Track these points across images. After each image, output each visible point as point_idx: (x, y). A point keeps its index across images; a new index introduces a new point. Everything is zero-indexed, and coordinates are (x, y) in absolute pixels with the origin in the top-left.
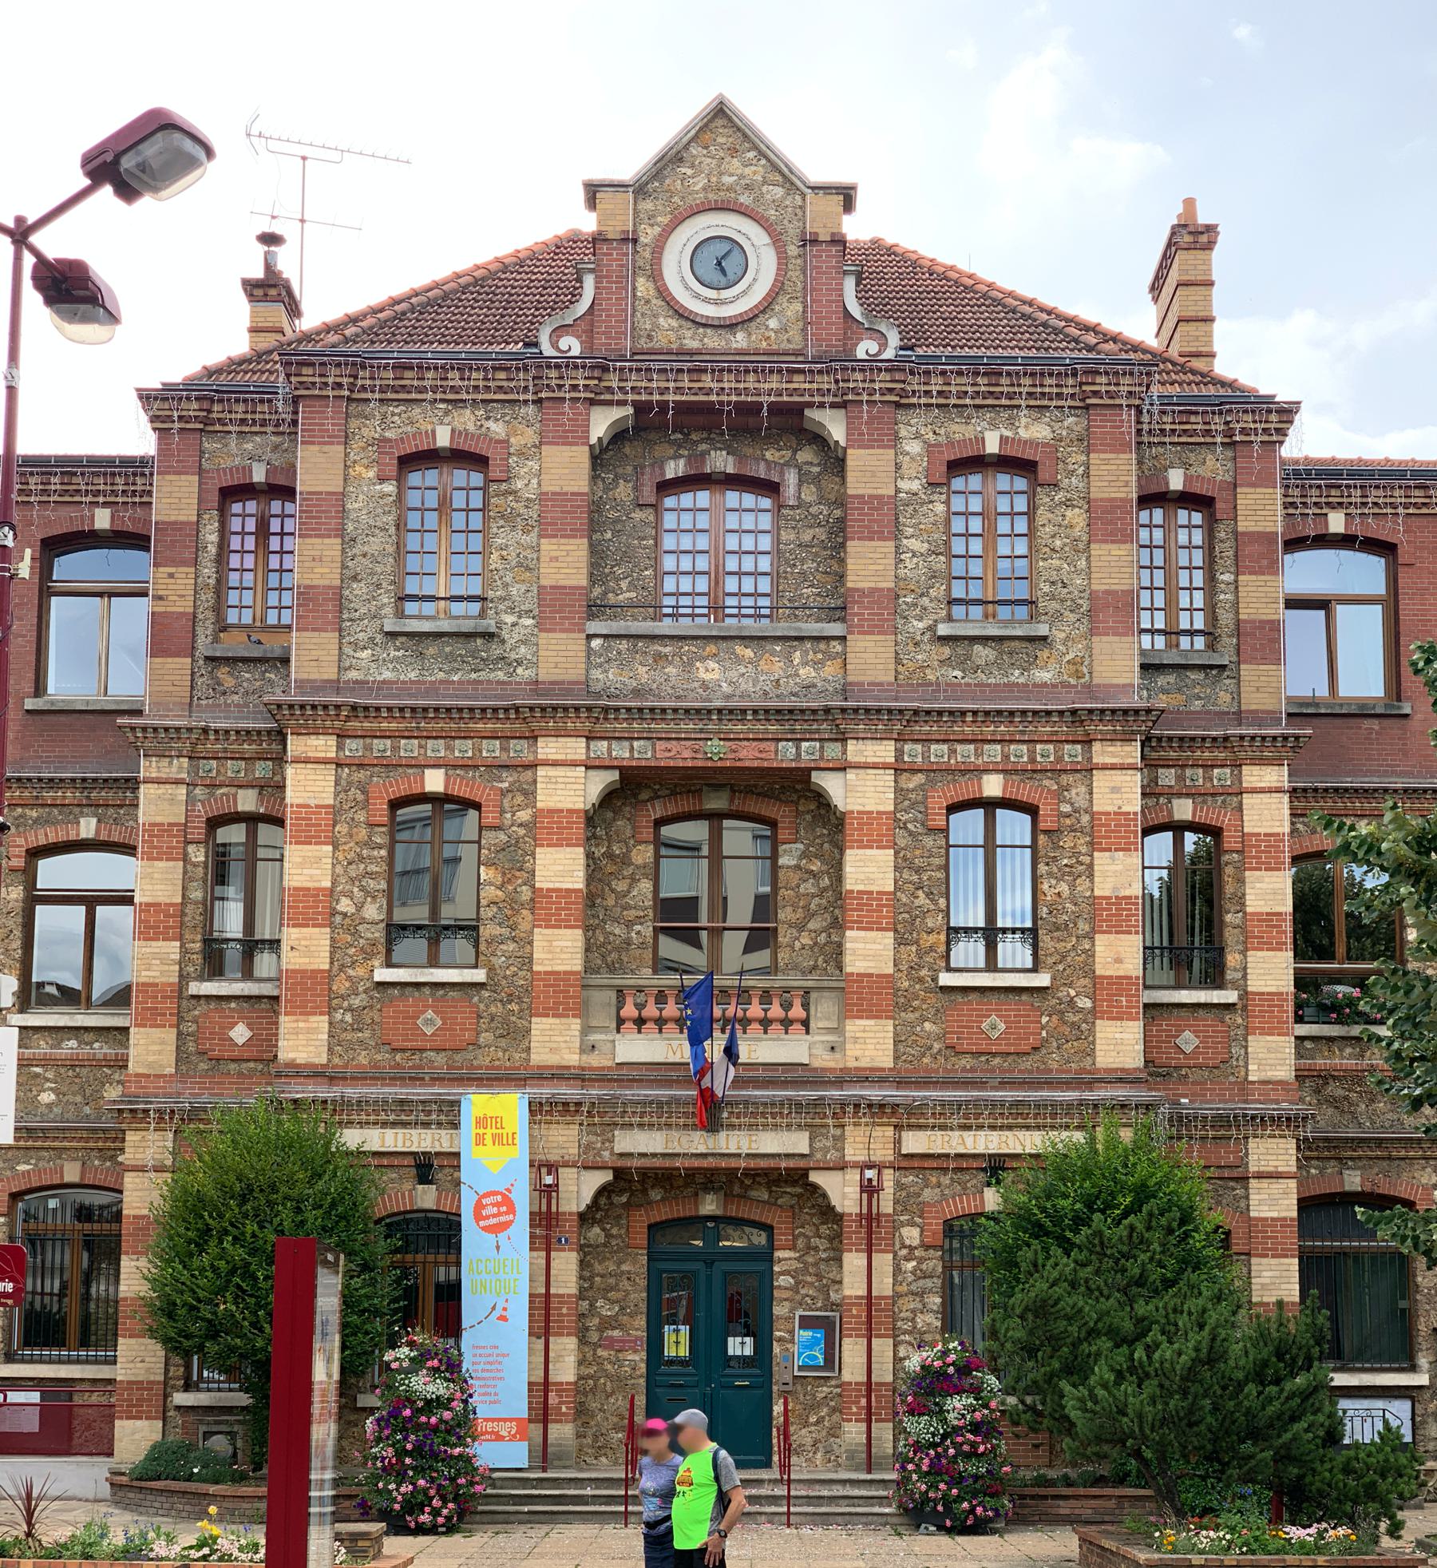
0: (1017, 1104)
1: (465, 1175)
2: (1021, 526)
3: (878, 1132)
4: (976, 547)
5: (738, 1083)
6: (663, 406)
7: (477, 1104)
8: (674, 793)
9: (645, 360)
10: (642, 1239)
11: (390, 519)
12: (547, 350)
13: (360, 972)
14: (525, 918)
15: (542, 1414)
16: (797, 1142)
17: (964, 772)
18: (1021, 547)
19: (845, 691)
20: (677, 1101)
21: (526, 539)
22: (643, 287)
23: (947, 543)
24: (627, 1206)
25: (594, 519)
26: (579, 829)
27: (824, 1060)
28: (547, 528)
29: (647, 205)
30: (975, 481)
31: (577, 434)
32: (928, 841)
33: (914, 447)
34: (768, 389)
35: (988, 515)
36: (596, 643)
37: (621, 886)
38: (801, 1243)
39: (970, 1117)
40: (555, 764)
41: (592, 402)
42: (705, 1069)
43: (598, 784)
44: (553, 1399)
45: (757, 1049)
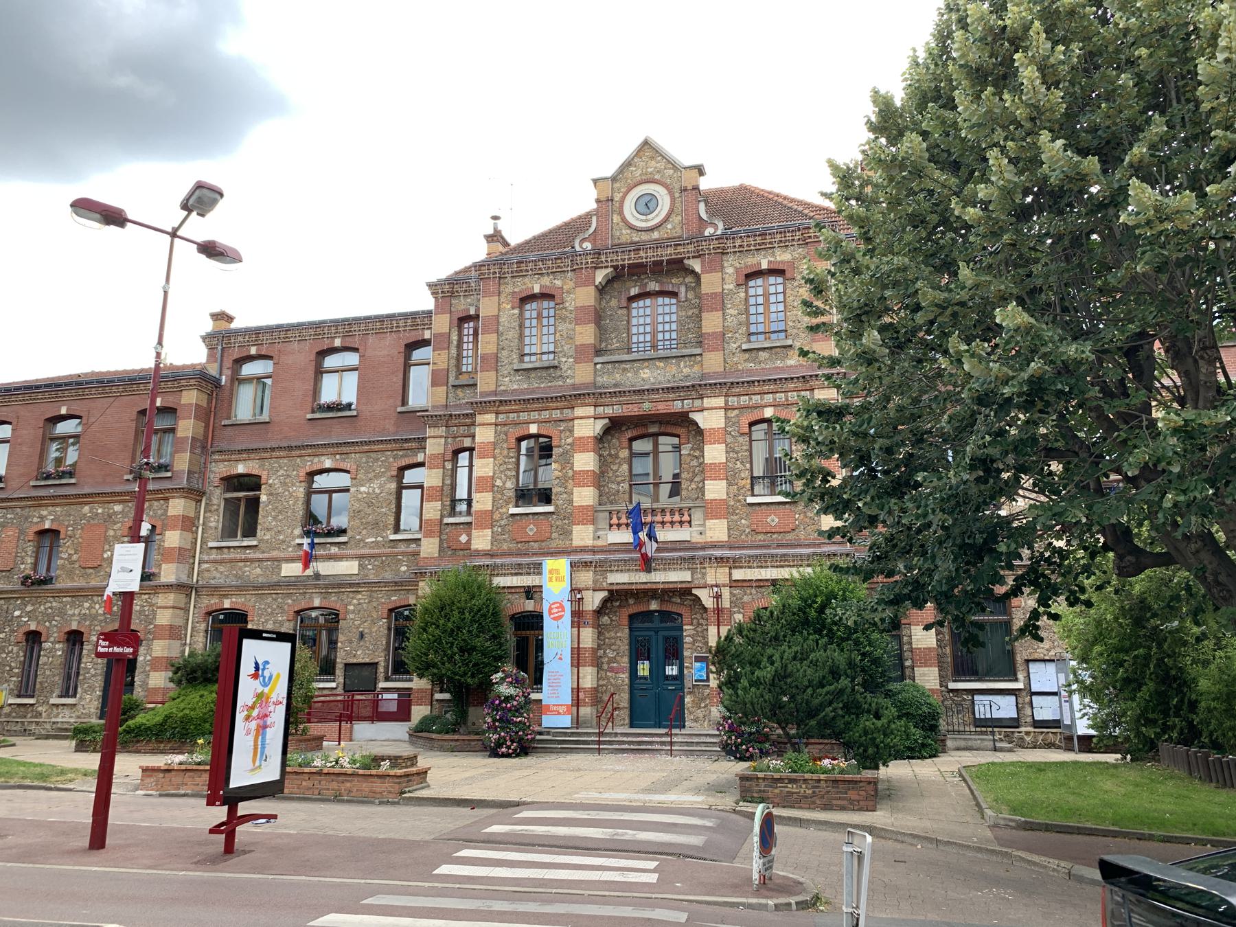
0: (784, 555)
1: (544, 595)
2: (781, 298)
3: (720, 570)
4: (761, 309)
5: (658, 550)
6: (623, 266)
7: (549, 564)
8: (636, 426)
9: (616, 248)
10: (626, 621)
11: (516, 324)
12: (578, 248)
13: (504, 510)
14: (570, 483)
15: (577, 703)
16: (685, 576)
17: (756, 408)
18: (781, 307)
19: (702, 377)
20: (632, 559)
21: (570, 326)
22: (616, 218)
23: (747, 310)
24: (620, 606)
25: (598, 318)
26: (591, 445)
27: (697, 538)
28: (578, 321)
29: (617, 185)
30: (759, 281)
31: (590, 281)
32: (741, 439)
33: (730, 270)
34: (666, 254)
35: (766, 295)
36: (598, 366)
37: (615, 468)
38: (695, 622)
39: (762, 562)
40: (582, 418)
41: (596, 268)
42: (639, 545)
43: (599, 425)
44: (581, 695)
45: (663, 535)
